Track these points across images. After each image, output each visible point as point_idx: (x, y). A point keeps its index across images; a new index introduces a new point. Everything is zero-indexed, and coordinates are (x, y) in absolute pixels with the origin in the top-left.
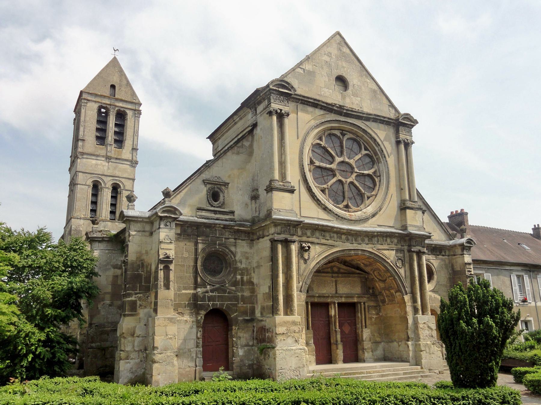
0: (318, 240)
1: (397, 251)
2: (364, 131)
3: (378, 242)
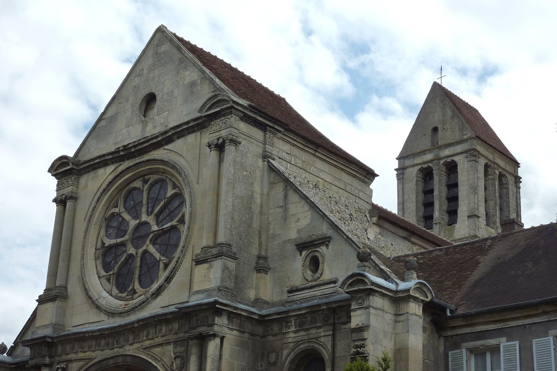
0: (76, 355)
1: (176, 343)
2: (163, 162)
3: (147, 335)
